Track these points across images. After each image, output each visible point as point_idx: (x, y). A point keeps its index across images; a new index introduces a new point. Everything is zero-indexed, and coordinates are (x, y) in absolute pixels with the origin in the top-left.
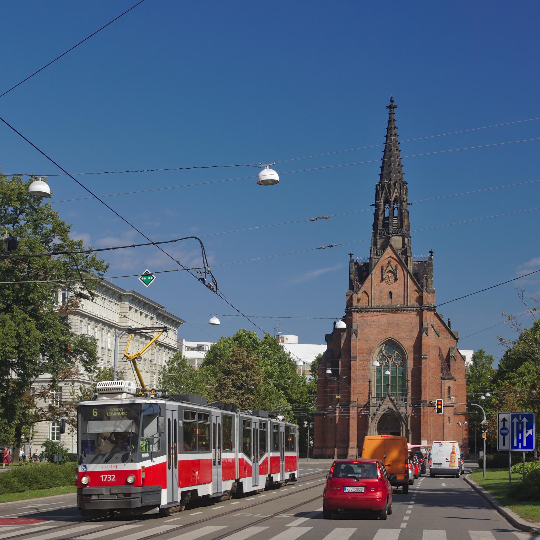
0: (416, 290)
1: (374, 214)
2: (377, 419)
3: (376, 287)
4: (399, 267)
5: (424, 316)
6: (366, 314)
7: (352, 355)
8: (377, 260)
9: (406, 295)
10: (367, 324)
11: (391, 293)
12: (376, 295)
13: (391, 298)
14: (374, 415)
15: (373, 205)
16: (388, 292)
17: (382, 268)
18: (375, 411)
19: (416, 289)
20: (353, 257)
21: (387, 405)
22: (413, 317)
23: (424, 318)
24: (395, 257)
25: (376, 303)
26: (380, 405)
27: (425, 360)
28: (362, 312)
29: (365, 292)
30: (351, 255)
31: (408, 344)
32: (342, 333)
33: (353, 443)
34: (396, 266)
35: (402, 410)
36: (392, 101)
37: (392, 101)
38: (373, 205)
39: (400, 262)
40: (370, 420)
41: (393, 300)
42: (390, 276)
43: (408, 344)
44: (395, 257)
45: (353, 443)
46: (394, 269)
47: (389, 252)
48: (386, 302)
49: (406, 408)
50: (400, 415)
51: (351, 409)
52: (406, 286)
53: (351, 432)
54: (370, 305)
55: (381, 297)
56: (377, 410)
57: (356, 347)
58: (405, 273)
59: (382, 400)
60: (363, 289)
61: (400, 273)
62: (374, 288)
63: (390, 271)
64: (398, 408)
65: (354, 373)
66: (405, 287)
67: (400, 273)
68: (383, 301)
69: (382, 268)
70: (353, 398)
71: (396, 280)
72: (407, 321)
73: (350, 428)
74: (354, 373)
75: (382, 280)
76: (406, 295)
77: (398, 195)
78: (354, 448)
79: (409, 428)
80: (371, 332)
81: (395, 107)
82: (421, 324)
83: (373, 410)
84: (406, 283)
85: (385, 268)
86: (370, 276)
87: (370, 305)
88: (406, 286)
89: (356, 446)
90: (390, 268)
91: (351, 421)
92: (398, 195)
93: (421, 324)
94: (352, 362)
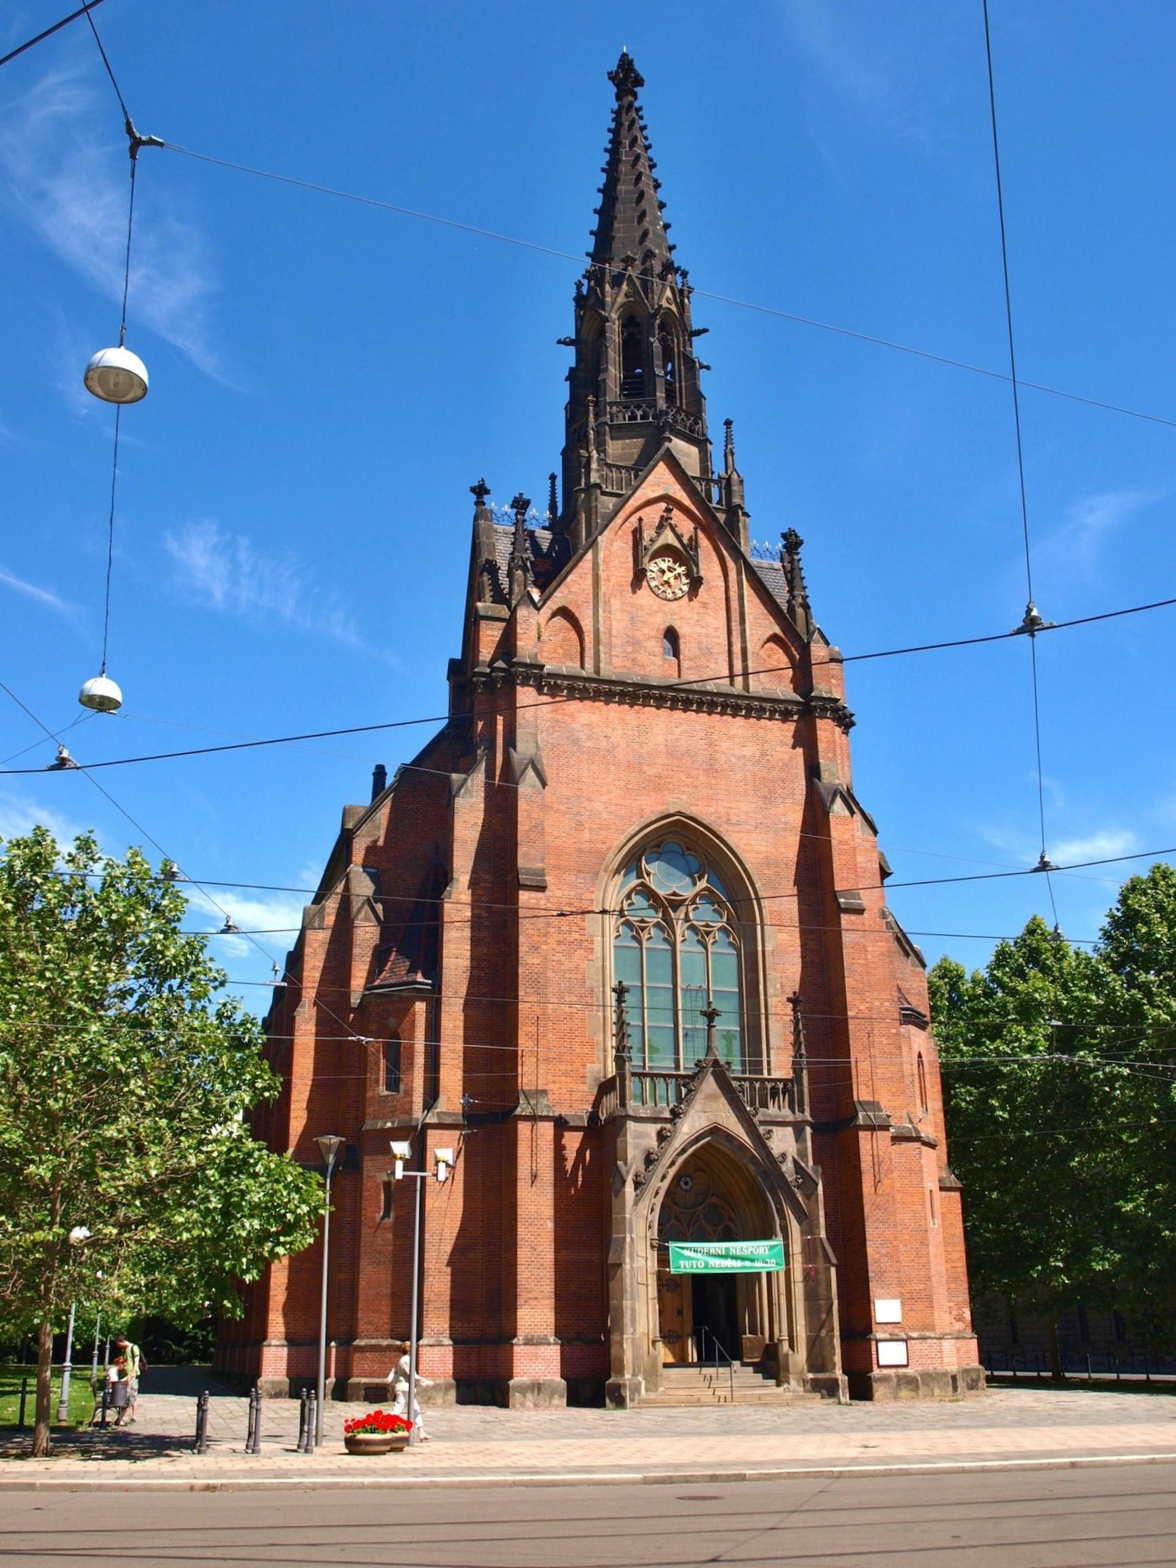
0: (774, 638)
2: (659, 1184)
3: (615, 604)
4: (704, 542)
6: (575, 705)
7: (522, 863)
8: (611, 502)
9: (737, 648)
10: (575, 742)
11: (671, 635)
12: (614, 632)
13: (676, 654)
14: (649, 1160)
16: (664, 627)
17: (637, 533)
18: (653, 1143)
19: (777, 630)
21: (708, 1112)
22: (780, 733)
23: (822, 747)
24: (687, 502)
25: (615, 661)
26: (676, 1114)
27: (853, 917)
28: (554, 691)
29: (565, 613)
30: (480, 491)
31: (765, 842)
32: (455, 776)
33: (536, 1313)
34: (694, 540)
35: (782, 1142)
36: (626, 64)
37: (626, 64)
39: (707, 522)
40: (629, 1188)
41: (685, 664)
42: (664, 566)
43: (765, 842)
44: (687, 502)
45: (536, 1313)
46: (686, 541)
47: (660, 480)
48: (656, 667)
49: (799, 1135)
50: (771, 1163)
51: (524, 1128)
52: (735, 616)
53: (523, 1254)
54: (589, 665)
55: (635, 643)
56: (662, 1137)
57: (540, 828)
58: (731, 565)
59: (686, 1085)
60: (560, 598)
61: (709, 566)
62: (607, 603)
63: (666, 551)
64: (762, 1129)
65: (535, 948)
66: (734, 620)
67: (709, 566)
68: (642, 658)
69: (637, 533)
70: (528, 1075)
71: (696, 583)
72: (747, 752)
73: (522, 1231)
74: (535, 948)
75: (639, 577)
76: (737, 648)
77: (673, 308)
79: (823, 1235)
80: (589, 780)
82: (813, 770)
83: (639, 1135)
84: (735, 605)
85: (648, 533)
86: (589, 556)
87: (589, 665)
88: (735, 616)
90: (668, 537)
91: (524, 1192)
92: (673, 308)
93: (813, 770)
94: (524, 897)
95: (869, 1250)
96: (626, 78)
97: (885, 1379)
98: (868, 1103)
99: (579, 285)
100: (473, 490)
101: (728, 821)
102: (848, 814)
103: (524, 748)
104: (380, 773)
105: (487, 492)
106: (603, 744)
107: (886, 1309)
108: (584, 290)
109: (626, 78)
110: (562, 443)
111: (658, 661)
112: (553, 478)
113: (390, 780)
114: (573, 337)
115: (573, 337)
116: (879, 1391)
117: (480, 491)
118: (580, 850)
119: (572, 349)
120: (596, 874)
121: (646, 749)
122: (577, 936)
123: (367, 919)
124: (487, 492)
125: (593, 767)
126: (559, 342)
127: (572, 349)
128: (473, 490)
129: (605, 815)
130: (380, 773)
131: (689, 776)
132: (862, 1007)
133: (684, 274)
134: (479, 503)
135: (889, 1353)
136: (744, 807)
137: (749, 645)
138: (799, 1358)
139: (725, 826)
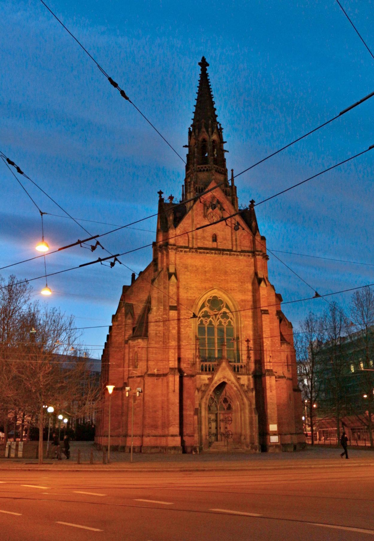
1: (187, 155)
5: (259, 264)
9: (234, 238)
15: (186, 146)
18: (207, 382)
20: (163, 196)
30: (160, 193)
36: (203, 59)
37: (203, 59)
38: (186, 146)
41: (219, 244)
72: (237, 269)
76: (234, 238)
78: (176, 436)
81: (208, 65)
86: (190, 212)
89: (178, 433)
95: (268, 411)
96: (204, 64)
97: (272, 446)
98: (269, 370)
99: (190, 128)
100: (158, 193)
101: (231, 290)
102: (265, 286)
103: (172, 270)
104: (133, 275)
105: (163, 193)
106: (195, 268)
107: (273, 427)
108: (191, 130)
109: (204, 64)
110: (185, 177)
111: (211, 243)
112: (183, 186)
113: (137, 277)
114: (188, 145)
115: (188, 145)
116: (270, 450)
117: (160, 193)
118: (187, 299)
119: (187, 149)
120: (192, 306)
121: (207, 269)
122: (186, 324)
123: (129, 319)
124: (163, 193)
125: (192, 275)
126: (184, 147)
127: (187, 149)
128: (158, 193)
129: (195, 289)
130: (133, 275)
131: (219, 276)
132: (268, 343)
133: (220, 125)
134: (160, 196)
135: (274, 439)
136: (235, 285)
137: (238, 238)
138: (248, 440)
139: (230, 291)
